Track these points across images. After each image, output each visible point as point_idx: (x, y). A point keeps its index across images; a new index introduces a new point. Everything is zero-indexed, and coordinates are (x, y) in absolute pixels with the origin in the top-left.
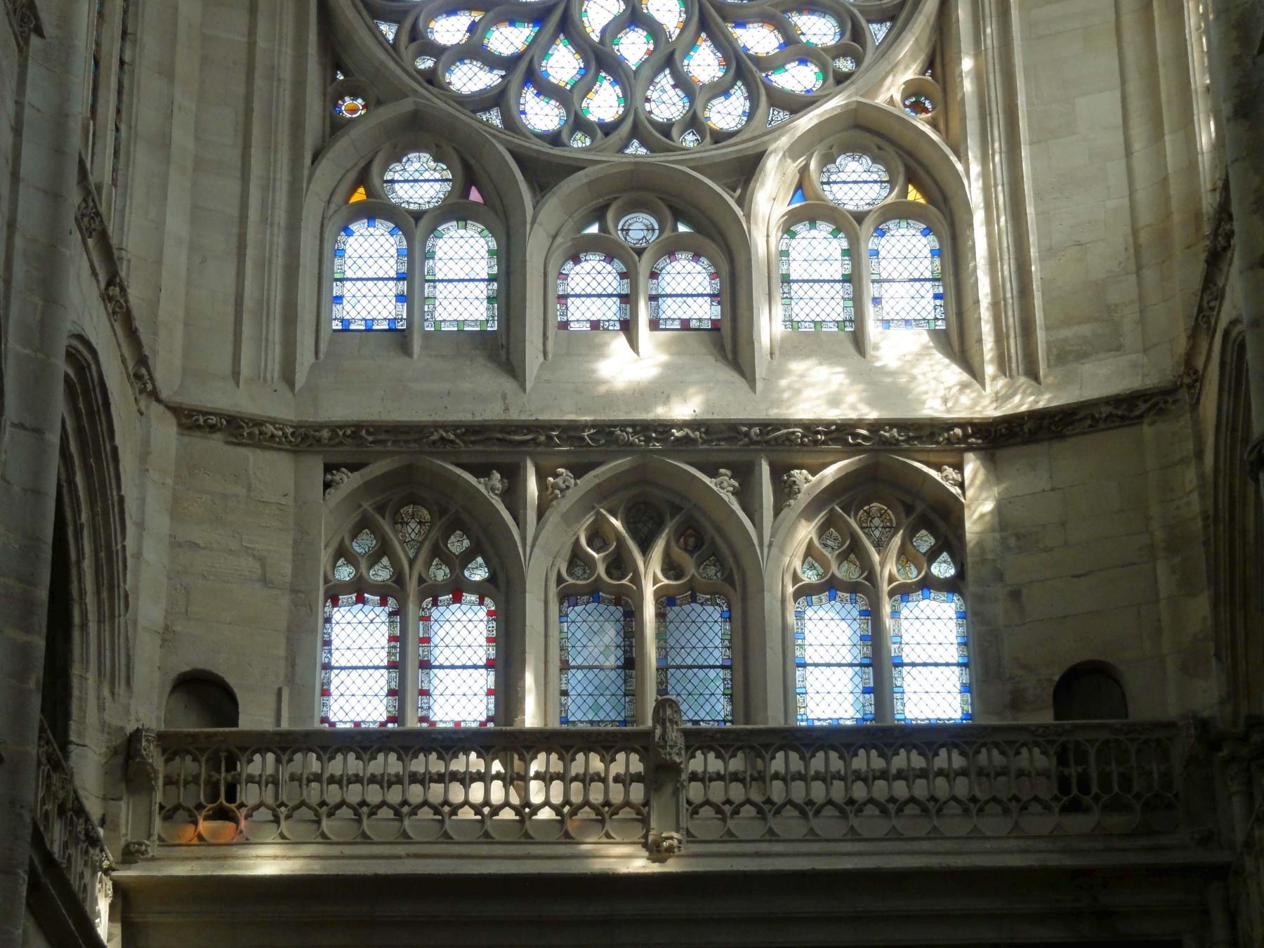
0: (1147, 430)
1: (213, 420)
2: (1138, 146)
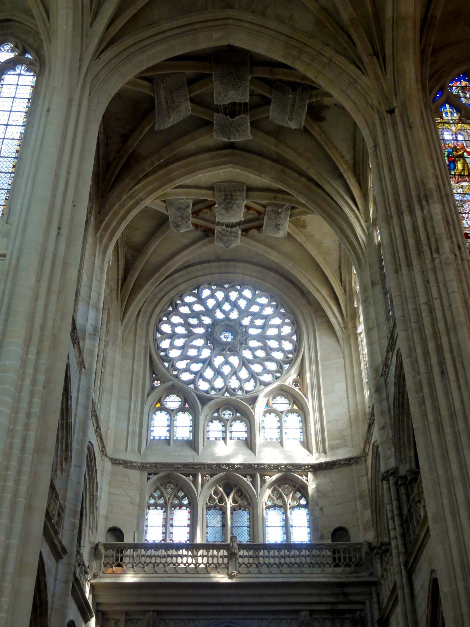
0: (354, 467)
1: (120, 462)
2: (350, 396)
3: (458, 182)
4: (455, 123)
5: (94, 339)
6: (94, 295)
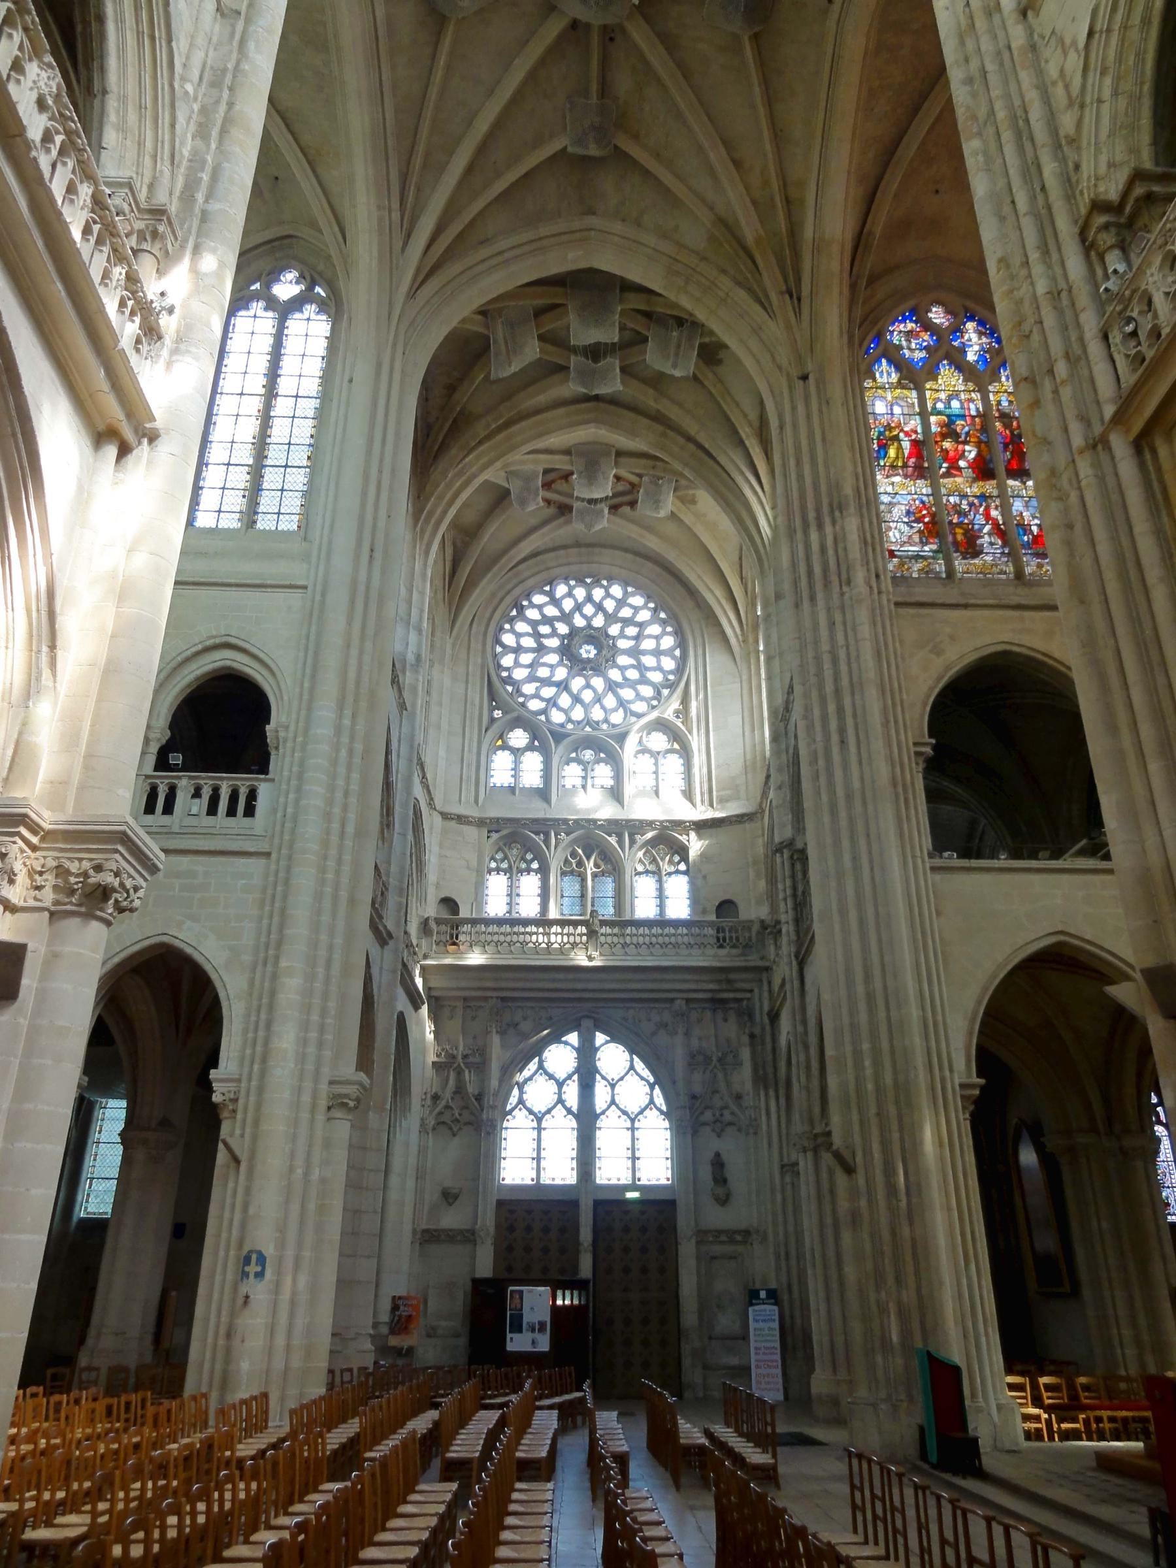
0: (747, 825)
3: (888, 477)
4: (893, 387)
5: (417, 672)
6: (415, 612)
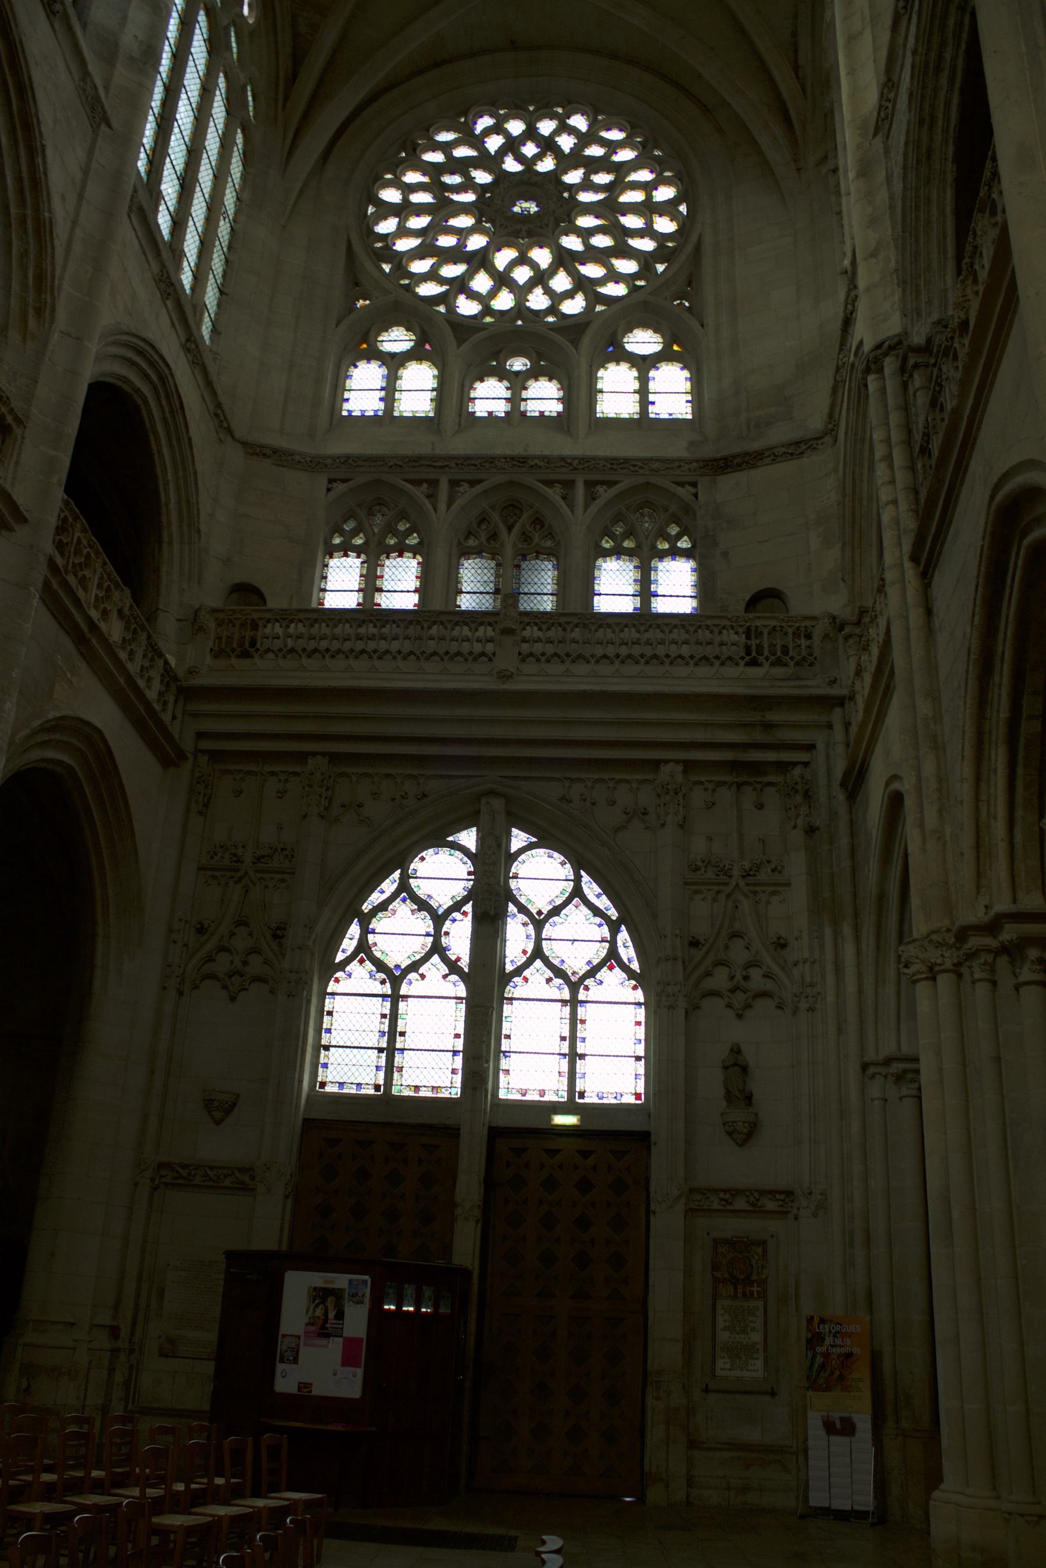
1: (265, 451)
